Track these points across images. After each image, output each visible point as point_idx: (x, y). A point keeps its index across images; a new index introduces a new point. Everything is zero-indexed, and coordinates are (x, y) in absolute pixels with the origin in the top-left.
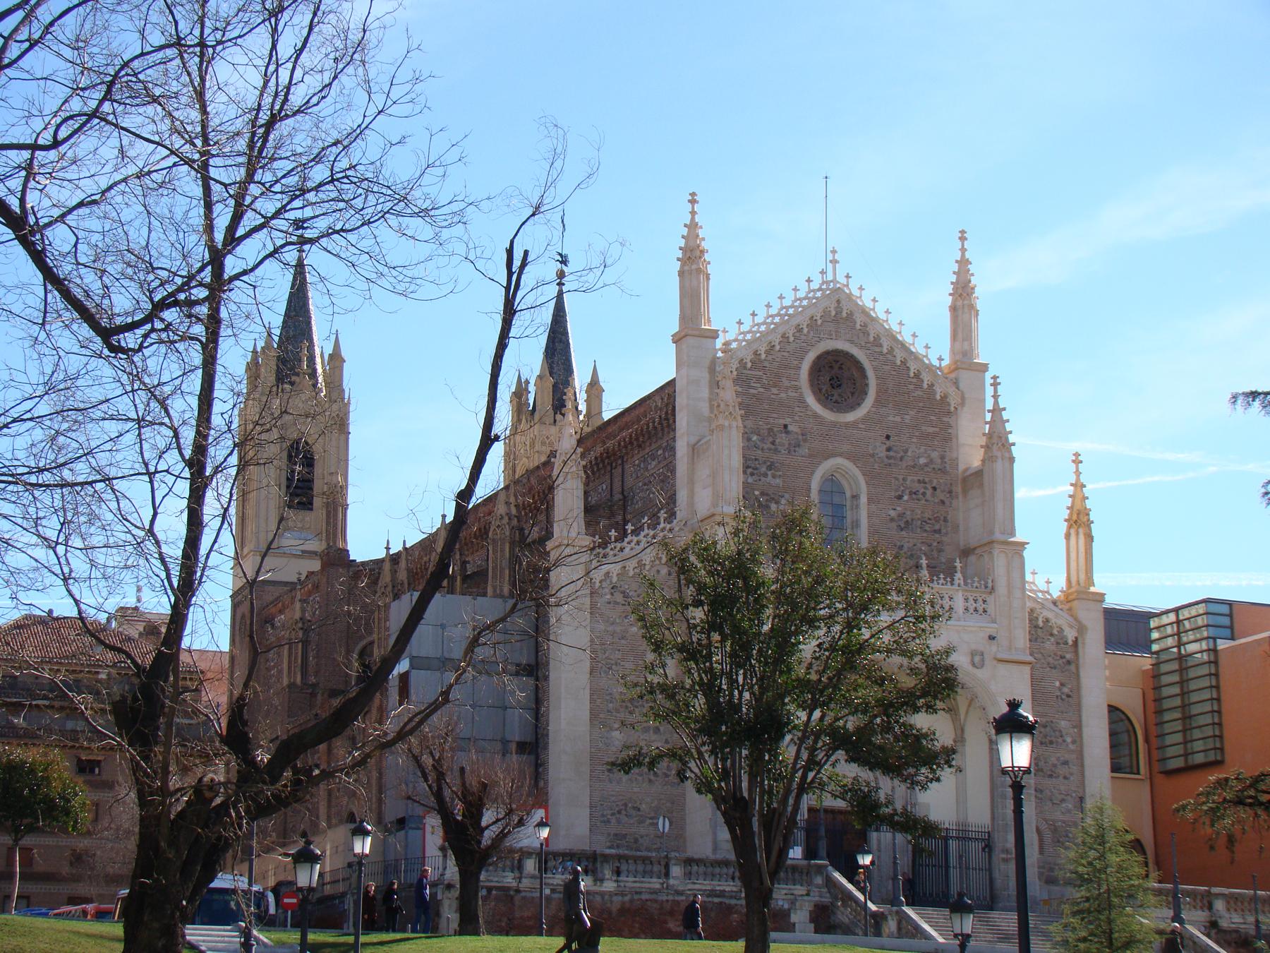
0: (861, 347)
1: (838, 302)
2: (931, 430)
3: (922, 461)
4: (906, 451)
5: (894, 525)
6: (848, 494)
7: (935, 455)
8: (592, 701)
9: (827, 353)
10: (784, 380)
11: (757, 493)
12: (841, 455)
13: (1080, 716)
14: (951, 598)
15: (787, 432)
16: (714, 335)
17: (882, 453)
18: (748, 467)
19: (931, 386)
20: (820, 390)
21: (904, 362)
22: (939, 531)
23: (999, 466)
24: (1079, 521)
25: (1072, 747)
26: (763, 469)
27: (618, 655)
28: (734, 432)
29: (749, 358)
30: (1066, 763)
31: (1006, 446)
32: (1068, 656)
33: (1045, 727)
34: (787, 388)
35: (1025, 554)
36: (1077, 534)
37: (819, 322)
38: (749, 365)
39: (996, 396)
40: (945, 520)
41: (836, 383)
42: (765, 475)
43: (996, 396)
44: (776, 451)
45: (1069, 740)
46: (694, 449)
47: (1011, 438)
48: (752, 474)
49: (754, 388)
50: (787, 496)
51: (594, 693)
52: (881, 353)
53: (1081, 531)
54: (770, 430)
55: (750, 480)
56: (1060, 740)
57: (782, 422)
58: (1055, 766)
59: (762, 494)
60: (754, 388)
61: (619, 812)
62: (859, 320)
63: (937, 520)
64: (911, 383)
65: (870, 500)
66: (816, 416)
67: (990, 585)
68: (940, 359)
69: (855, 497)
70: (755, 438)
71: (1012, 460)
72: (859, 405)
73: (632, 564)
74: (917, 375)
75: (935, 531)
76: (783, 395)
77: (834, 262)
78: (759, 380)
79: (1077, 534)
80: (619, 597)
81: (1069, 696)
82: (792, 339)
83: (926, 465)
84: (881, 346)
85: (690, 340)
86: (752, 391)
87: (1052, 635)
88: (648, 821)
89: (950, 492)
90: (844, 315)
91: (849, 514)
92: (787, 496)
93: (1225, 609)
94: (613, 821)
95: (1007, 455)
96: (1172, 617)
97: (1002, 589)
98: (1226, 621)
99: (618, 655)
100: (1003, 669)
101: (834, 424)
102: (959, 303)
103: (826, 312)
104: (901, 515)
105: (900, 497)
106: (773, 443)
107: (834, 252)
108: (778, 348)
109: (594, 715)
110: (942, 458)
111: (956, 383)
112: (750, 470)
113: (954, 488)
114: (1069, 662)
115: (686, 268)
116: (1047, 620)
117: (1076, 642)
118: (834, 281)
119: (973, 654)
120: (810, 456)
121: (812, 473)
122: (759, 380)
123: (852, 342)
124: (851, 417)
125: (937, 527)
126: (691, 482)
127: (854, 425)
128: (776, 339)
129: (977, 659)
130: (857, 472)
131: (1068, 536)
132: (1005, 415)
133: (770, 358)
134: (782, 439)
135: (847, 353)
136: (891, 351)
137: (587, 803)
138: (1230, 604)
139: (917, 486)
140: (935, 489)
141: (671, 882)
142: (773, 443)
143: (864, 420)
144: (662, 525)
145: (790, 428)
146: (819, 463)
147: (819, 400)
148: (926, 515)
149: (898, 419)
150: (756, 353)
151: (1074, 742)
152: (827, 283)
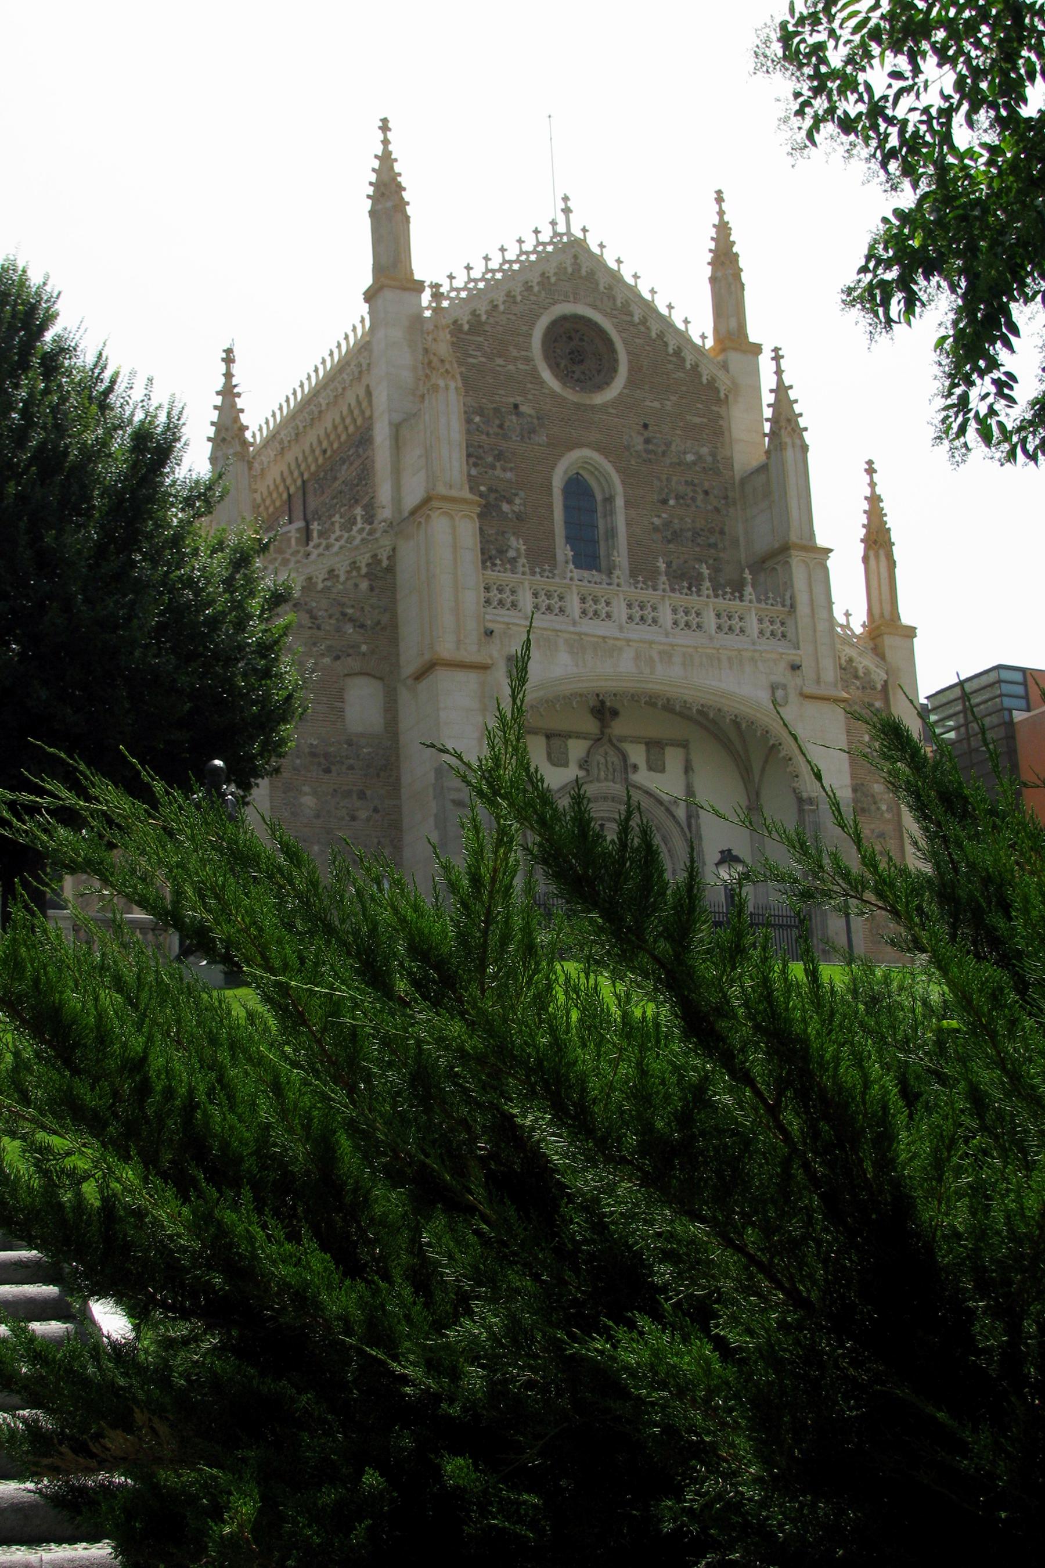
0: (606, 314)
1: (575, 257)
2: (697, 420)
3: (690, 458)
4: (668, 445)
6: (599, 497)
7: (704, 450)
9: (564, 318)
10: (511, 348)
11: (482, 488)
12: (588, 445)
16: (419, 287)
19: (695, 367)
20: (558, 365)
21: (661, 336)
23: (789, 454)
24: (878, 541)
25: (887, 816)
26: (490, 459)
28: (452, 396)
29: (466, 319)
30: (882, 835)
31: (798, 432)
34: (516, 359)
35: (829, 563)
36: (877, 557)
37: (553, 280)
38: (466, 327)
39: (779, 372)
40: (722, 532)
41: (577, 357)
42: (493, 467)
43: (779, 372)
45: (884, 808)
46: (396, 430)
47: (802, 422)
48: (475, 465)
49: (474, 357)
50: (522, 494)
52: (631, 323)
53: (882, 553)
54: (497, 410)
55: (474, 472)
56: (873, 807)
57: (512, 400)
59: (490, 490)
60: (471, 356)
62: (603, 282)
63: (712, 531)
64: (670, 362)
65: (628, 504)
66: (554, 395)
67: (788, 602)
68: (703, 337)
69: (609, 500)
70: (477, 419)
71: (805, 448)
72: (608, 384)
73: (320, 576)
74: (678, 352)
75: (710, 545)
76: (511, 367)
77: (567, 211)
78: (479, 347)
79: (877, 557)
82: (519, 298)
83: (694, 463)
84: (632, 316)
85: (388, 294)
87: (857, 677)
89: (726, 498)
91: (601, 523)
92: (522, 494)
93: (1018, 677)
95: (798, 442)
96: (958, 692)
97: (803, 608)
98: (1020, 690)
100: (811, 709)
101: (578, 406)
102: (719, 274)
103: (561, 270)
104: (667, 524)
105: (665, 502)
107: (566, 199)
108: (502, 308)
110: (714, 455)
111: (725, 366)
112: (472, 460)
115: (380, 207)
118: (568, 233)
119: (774, 688)
121: (553, 468)
122: (479, 347)
123: (595, 307)
125: (712, 540)
126: (397, 471)
127: (605, 406)
128: (500, 298)
129: (779, 693)
130: (609, 468)
131: (865, 559)
132: (792, 394)
136: (644, 321)
138: (1023, 671)
139: (682, 489)
142: (501, 426)
143: (616, 402)
144: (359, 525)
145: (523, 409)
146: (561, 456)
147: (556, 376)
149: (656, 404)
150: (474, 313)
152: (561, 235)
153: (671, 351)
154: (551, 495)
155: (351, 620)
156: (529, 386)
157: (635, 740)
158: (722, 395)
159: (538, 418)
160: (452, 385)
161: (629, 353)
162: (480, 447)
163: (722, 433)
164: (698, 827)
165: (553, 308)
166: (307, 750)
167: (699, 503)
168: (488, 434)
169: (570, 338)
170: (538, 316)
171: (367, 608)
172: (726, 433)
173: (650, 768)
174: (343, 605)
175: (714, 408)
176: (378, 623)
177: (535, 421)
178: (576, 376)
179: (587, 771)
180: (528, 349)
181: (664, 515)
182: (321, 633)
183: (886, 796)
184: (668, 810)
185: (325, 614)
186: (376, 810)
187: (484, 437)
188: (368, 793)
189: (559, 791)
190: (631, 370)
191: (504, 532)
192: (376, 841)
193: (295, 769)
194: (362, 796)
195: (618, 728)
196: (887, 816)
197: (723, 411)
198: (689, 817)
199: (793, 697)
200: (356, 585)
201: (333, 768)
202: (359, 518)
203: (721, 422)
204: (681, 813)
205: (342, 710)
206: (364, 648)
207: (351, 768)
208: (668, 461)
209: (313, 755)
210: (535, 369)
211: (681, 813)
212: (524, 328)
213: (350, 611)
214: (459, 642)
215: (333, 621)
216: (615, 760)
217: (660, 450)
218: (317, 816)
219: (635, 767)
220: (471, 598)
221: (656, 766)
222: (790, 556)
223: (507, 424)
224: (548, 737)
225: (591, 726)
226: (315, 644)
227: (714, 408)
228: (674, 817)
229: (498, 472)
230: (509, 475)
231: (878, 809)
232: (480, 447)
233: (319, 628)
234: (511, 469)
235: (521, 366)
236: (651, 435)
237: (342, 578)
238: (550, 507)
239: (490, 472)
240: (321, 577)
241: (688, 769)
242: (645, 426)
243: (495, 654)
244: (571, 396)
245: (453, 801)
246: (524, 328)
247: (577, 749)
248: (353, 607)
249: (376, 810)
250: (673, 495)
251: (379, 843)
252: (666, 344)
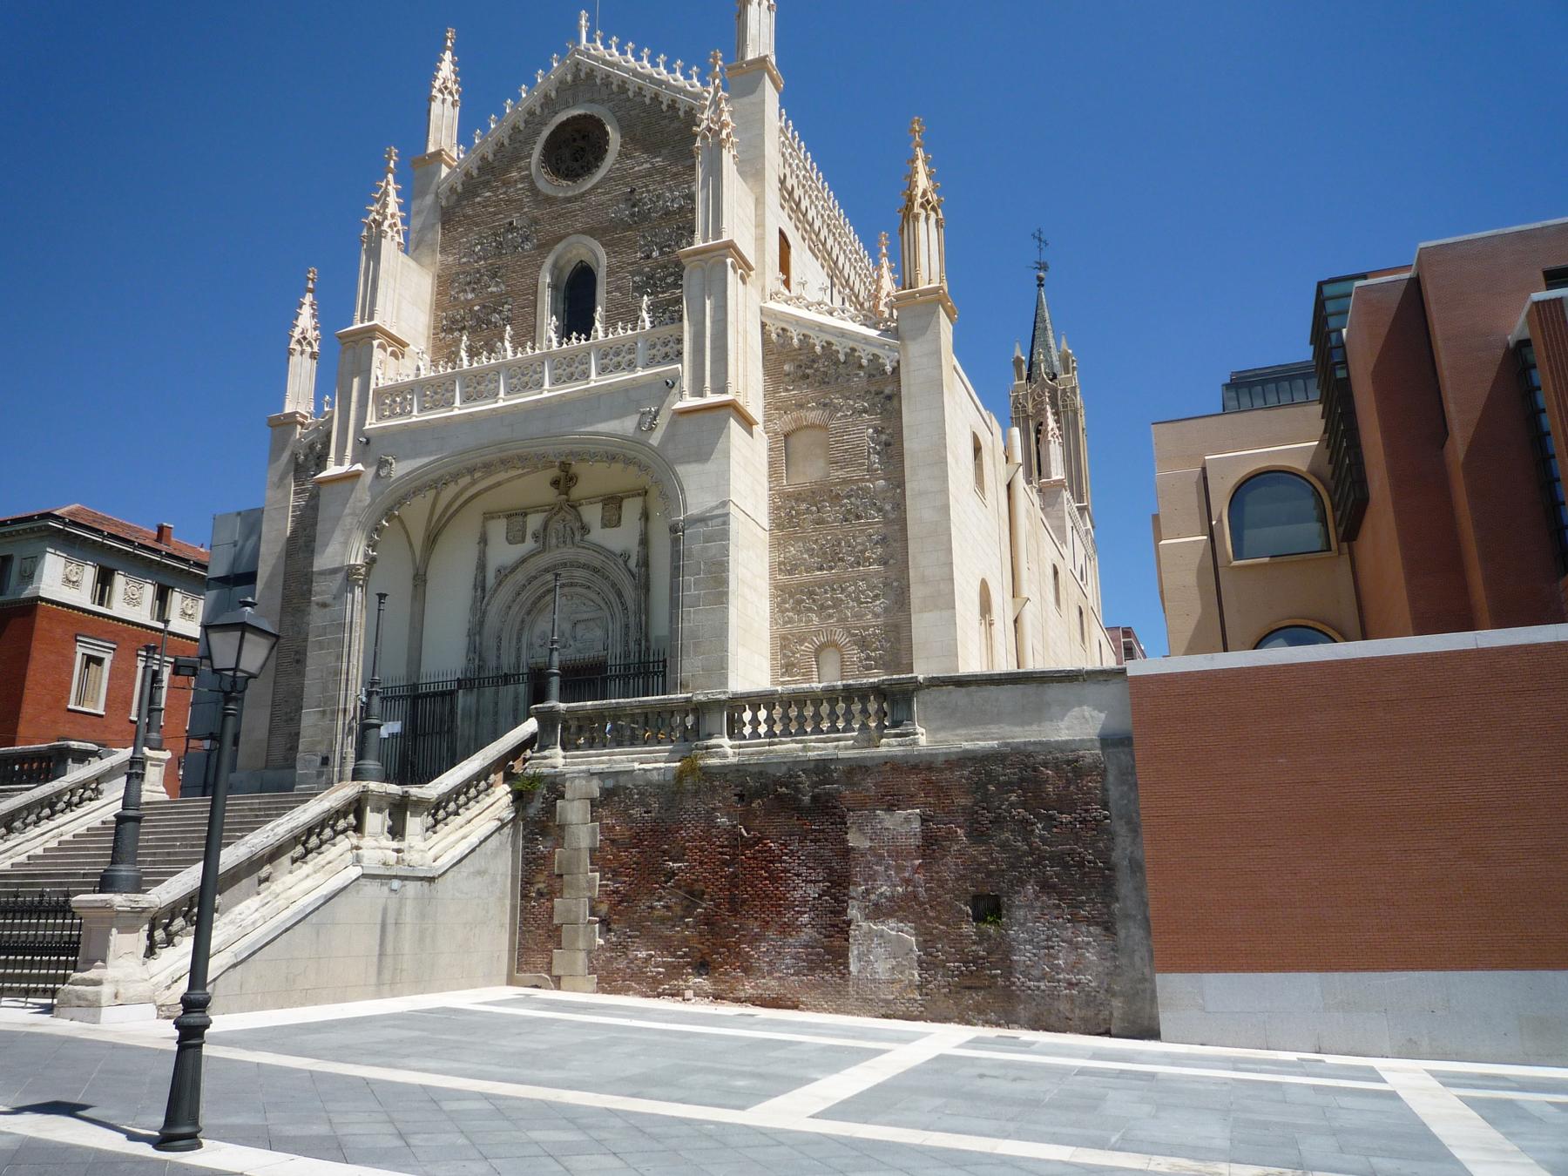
32: (887, 391)
33: (849, 497)
38: (475, 173)
48: (474, 290)
52: (629, 99)
58: (863, 552)
59: (484, 307)
87: (861, 367)
90: (583, 75)
105: (648, 257)
114: (889, 398)
116: (853, 350)
117: (896, 370)
121: (540, 267)
123: (592, 101)
124: (589, 183)
153: (664, 107)
157: (591, 500)
173: (604, 526)
195: (577, 492)
204: (632, 563)
219: (585, 529)
221: (612, 520)
224: (509, 517)
225: (550, 495)
241: (646, 516)
242: (633, 191)
247: (534, 522)
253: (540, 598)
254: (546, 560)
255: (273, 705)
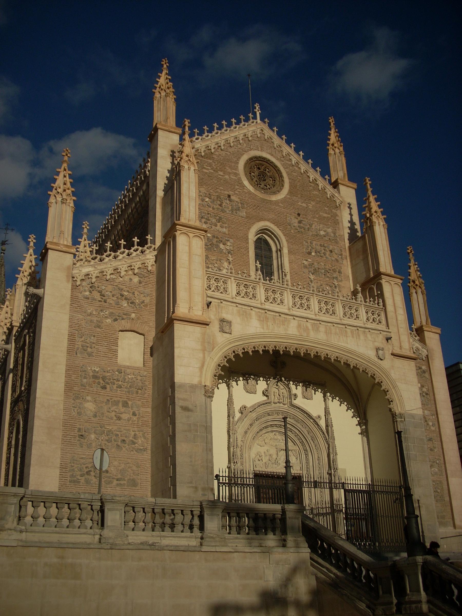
0: (278, 159)
2: (325, 215)
3: (322, 233)
4: (311, 225)
5: (306, 271)
6: (274, 249)
7: (330, 230)
8: (68, 376)
10: (227, 168)
11: (209, 235)
13: (436, 408)
14: (357, 311)
15: (230, 200)
17: (295, 222)
18: (202, 218)
22: (336, 278)
25: (433, 428)
26: (214, 221)
27: (93, 339)
32: (424, 367)
34: (230, 173)
36: (416, 293)
40: (340, 272)
44: (223, 211)
48: (206, 223)
49: (208, 169)
51: (70, 369)
54: (218, 197)
59: (214, 237)
61: (88, 473)
63: (334, 271)
64: (311, 186)
65: (290, 252)
66: (250, 193)
70: (207, 199)
75: (334, 278)
76: (227, 177)
78: (210, 165)
80: (97, 295)
81: (427, 394)
86: (205, 170)
88: (115, 482)
89: (341, 255)
94: (82, 480)
99: (93, 339)
100: (399, 362)
101: (263, 200)
104: (311, 265)
105: (310, 253)
106: (220, 205)
109: (69, 387)
112: (203, 220)
113: (344, 254)
114: (424, 372)
119: (377, 349)
120: (247, 217)
121: (249, 229)
124: (274, 198)
125: (335, 276)
127: (277, 203)
129: (380, 352)
133: (217, 153)
134: (226, 202)
135: (269, 160)
137: (59, 465)
139: (318, 248)
140: (331, 251)
141: (106, 533)
142: (220, 205)
143: (283, 201)
145: (232, 197)
146: (254, 223)
148: (327, 267)
149: (304, 205)
151: (433, 425)
153: (311, 180)
154: (248, 243)
155: (126, 299)
156: (238, 187)
158: (338, 204)
159: (241, 204)
160: (192, 168)
161: (289, 179)
162: (208, 214)
163: (338, 223)
164: (333, 432)
165: (250, 152)
166: (91, 374)
167: (327, 255)
168: (213, 208)
169: (259, 169)
170: (242, 155)
171: (136, 293)
172: (340, 224)
173: (304, 397)
174: (122, 289)
175: (333, 210)
176: (143, 302)
177: (240, 205)
178: (262, 186)
179: (267, 396)
180: (237, 169)
181: (309, 260)
182: (106, 305)
183: (431, 417)
184: (315, 421)
185: (110, 294)
186: (134, 414)
187: (211, 209)
188: (130, 403)
189: (250, 407)
190: (290, 186)
191: (220, 260)
192: (133, 433)
193: (82, 385)
194: (125, 404)
196: (433, 428)
197: (338, 212)
198: (327, 426)
199: (388, 355)
200: (131, 279)
201: (108, 386)
202: (136, 243)
203: (337, 218)
204: (322, 423)
205: (116, 351)
206: (133, 315)
207: (120, 387)
208: (311, 233)
209: (95, 377)
210: (240, 179)
211: (322, 423)
212: (235, 159)
213: (126, 293)
214: (190, 308)
215: (115, 298)
216: (284, 391)
217: (306, 227)
218: (95, 416)
219: (295, 395)
220: (199, 284)
222: (381, 279)
223: (224, 204)
226: (102, 311)
227: (333, 210)
228: (317, 424)
229: (218, 228)
230: (224, 230)
231: (428, 424)
232: (208, 214)
233: (105, 302)
234: (226, 228)
235: (231, 177)
236: (302, 219)
237: (123, 273)
238: (248, 248)
239: (214, 227)
240: (109, 272)
243: (212, 317)
244: (260, 195)
245: (182, 407)
246: (235, 159)
248: (128, 291)
249: (134, 414)
250: (314, 250)
251: (135, 435)
252: (309, 177)
253: (261, 430)
254: (268, 408)
255: (63, 467)
